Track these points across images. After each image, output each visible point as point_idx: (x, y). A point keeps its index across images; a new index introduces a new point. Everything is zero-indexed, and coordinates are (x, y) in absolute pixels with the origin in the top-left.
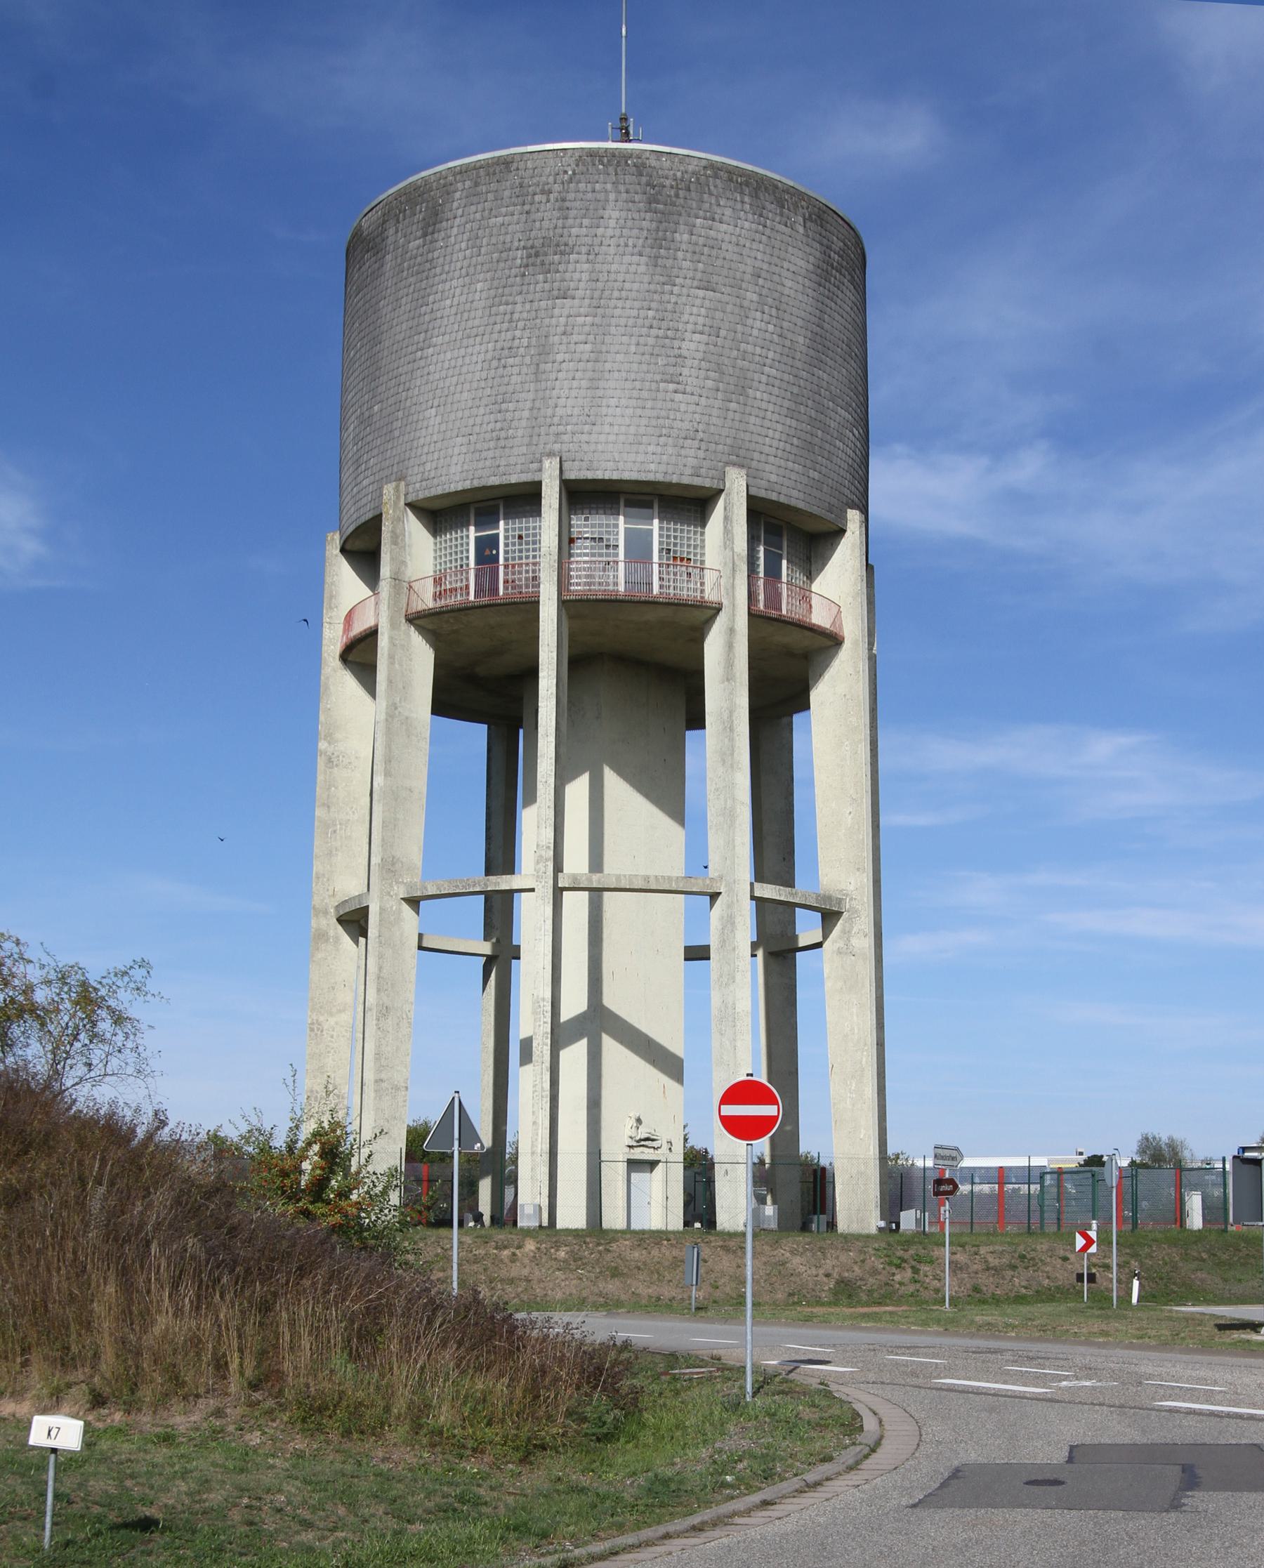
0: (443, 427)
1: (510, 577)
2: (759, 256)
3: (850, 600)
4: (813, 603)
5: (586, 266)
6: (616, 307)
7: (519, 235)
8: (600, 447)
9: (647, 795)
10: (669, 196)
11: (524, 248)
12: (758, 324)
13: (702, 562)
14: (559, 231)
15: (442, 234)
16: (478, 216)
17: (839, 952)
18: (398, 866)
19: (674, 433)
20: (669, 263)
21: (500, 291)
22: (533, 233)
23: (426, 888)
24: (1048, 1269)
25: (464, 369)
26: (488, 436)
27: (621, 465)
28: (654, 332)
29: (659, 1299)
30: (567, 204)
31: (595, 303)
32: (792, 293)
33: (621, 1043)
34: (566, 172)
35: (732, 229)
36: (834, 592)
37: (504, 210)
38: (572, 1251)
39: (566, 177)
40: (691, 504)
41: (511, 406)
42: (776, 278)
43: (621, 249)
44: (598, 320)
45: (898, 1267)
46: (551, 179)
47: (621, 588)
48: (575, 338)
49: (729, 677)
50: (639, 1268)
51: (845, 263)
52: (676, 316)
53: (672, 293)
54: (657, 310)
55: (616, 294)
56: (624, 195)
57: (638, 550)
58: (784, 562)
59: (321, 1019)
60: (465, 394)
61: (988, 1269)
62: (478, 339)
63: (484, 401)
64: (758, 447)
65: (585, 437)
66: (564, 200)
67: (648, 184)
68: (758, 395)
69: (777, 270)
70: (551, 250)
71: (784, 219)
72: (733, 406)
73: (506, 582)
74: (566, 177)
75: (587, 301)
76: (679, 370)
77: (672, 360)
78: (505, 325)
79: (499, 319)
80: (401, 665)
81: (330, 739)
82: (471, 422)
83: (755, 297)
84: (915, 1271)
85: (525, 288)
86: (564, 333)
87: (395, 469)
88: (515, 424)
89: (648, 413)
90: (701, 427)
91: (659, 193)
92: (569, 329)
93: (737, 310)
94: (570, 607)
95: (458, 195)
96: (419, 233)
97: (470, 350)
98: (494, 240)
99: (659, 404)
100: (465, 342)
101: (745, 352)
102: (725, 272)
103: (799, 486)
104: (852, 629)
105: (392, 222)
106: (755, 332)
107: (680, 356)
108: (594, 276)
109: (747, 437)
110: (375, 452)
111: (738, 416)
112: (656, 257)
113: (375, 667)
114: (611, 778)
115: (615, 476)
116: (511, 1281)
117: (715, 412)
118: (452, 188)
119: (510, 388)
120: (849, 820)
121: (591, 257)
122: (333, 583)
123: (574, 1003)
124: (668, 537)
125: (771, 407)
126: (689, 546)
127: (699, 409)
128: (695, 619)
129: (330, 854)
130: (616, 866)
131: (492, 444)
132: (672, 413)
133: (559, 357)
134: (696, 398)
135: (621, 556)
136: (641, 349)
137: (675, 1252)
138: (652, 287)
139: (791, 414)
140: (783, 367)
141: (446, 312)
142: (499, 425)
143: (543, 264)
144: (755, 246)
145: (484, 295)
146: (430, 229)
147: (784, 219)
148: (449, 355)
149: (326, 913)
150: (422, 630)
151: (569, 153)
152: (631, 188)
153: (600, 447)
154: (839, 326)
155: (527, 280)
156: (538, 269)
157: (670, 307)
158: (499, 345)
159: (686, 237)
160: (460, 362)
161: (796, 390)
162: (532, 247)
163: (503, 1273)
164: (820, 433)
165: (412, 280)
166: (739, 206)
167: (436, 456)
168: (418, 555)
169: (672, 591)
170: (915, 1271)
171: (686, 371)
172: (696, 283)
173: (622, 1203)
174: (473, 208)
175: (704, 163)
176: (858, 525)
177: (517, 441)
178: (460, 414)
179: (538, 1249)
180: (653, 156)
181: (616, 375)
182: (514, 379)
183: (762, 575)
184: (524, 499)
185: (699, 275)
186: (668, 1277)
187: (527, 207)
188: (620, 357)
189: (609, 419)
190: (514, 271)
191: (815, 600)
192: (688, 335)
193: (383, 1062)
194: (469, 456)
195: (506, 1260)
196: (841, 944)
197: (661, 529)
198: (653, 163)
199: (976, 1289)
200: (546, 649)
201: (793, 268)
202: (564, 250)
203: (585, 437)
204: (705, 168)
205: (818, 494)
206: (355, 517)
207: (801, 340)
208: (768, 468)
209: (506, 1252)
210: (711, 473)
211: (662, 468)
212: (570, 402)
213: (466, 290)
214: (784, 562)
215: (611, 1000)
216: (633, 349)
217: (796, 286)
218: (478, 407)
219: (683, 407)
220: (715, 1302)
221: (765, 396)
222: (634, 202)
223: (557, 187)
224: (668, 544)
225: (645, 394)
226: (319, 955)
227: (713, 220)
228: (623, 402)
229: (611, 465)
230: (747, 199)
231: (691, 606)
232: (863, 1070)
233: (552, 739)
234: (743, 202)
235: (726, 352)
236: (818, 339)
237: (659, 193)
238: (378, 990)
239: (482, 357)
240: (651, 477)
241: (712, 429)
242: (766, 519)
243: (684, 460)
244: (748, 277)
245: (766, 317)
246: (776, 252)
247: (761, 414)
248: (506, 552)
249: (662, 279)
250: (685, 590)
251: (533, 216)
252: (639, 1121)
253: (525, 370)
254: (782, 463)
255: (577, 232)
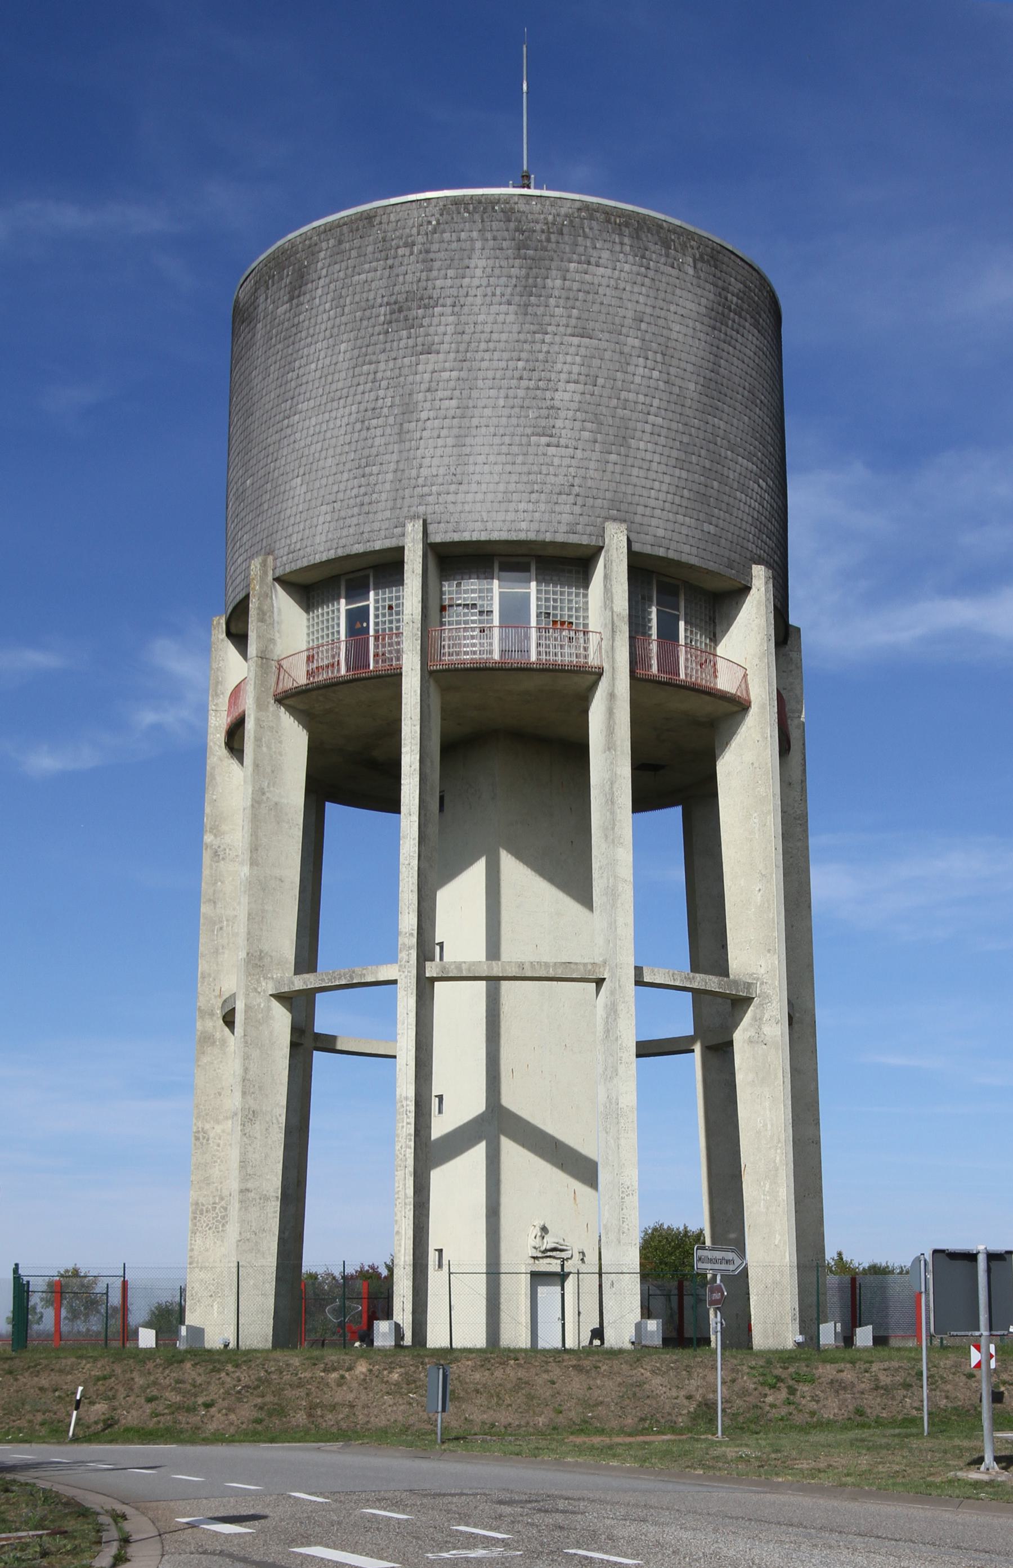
0: (309, 496)
1: (380, 650)
2: (642, 299)
3: (756, 661)
4: (719, 666)
5: (451, 319)
6: (483, 360)
7: (382, 291)
8: (467, 508)
9: (551, 880)
10: (541, 241)
11: (388, 304)
12: (640, 370)
13: (586, 625)
14: (423, 284)
15: (308, 296)
16: (342, 274)
17: (750, 1041)
18: (267, 960)
19: (547, 488)
20: (540, 310)
21: (364, 349)
22: (397, 288)
23: (293, 983)
24: (949, 1387)
25: (328, 435)
26: (352, 502)
27: (489, 525)
28: (524, 383)
29: (493, 1425)
30: (432, 255)
31: (460, 356)
32: (681, 338)
33: (523, 1146)
34: (430, 223)
35: (611, 272)
36: (741, 654)
37: (367, 266)
38: (406, 1373)
39: (430, 228)
40: (568, 564)
41: (375, 469)
42: (661, 322)
43: (488, 299)
44: (463, 374)
45: (773, 1387)
46: (415, 231)
47: (496, 656)
48: (440, 394)
49: (610, 746)
50: (477, 1391)
51: (745, 306)
52: (548, 366)
53: (543, 342)
54: (527, 361)
55: (483, 346)
56: (491, 243)
57: (514, 614)
58: (682, 624)
59: (207, 1126)
60: (329, 460)
61: (877, 1388)
62: (342, 401)
63: (348, 466)
64: (642, 500)
65: (451, 498)
66: (427, 252)
67: (517, 230)
68: (642, 445)
69: (663, 313)
70: (415, 305)
71: (670, 260)
72: (613, 457)
73: (376, 655)
74: (430, 228)
75: (452, 355)
76: (552, 422)
77: (544, 412)
78: (369, 385)
79: (362, 379)
80: (269, 747)
81: (216, 832)
82: (335, 488)
83: (637, 343)
84: (792, 1391)
85: (388, 345)
86: (429, 390)
87: (264, 544)
88: (377, 488)
89: (518, 468)
90: (577, 481)
91: (529, 238)
92: (434, 385)
93: (616, 357)
94: (434, 676)
95: (322, 255)
96: (286, 298)
97: (334, 414)
98: (357, 298)
99: (530, 459)
100: (329, 406)
101: (626, 400)
102: (602, 318)
103: (692, 541)
104: (761, 694)
105: (263, 289)
106: (638, 379)
107: (552, 407)
108: (460, 328)
109: (630, 490)
110: (248, 527)
111: (618, 469)
112: (526, 305)
113: (243, 751)
114: (508, 862)
115: (484, 537)
116: (333, 1408)
117: (592, 465)
118: (317, 248)
119: (374, 451)
120: (758, 898)
121: (456, 309)
122: (218, 669)
123: (461, 1100)
124: (547, 600)
125: (657, 458)
126: (570, 609)
127: (574, 462)
128: (577, 685)
129: (216, 952)
130: (515, 952)
131: (356, 510)
132: (544, 468)
133: (424, 415)
134: (571, 451)
135: (496, 622)
136: (511, 402)
137: (521, 1373)
138: (522, 337)
139: (681, 464)
140: (670, 415)
141: (311, 377)
142: (363, 490)
143: (406, 319)
144: (636, 289)
145: (348, 355)
146: (297, 293)
147: (670, 260)
148: (313, 421)
149: (212, 1014)
150: (292, 710)
151: (433, 202)
152: (499, 234)
153: (467, 508)
154: (738, 371)
155: (390, 337)
156: (401, 324)
157: (541, 356)
158: (362, 407)
159: (558, 283)
160: (324, 427)
161: (686, 439)
162: (395, 303)
163: (327, 1398)
164: (715, 484)
165: (280, 346)
166: (617, 248)
167: (302, 527)
168: (296, 636)
169: (574, 659)
170: (792, 1391)
171: (559, 423)
172: (569, 331)
173: (525, 1318)
174: (337, 267)
175: (577, 205)
176: (763, 580)
177: (381, 506)
178: (324, 481)
179: (370, 1371)
180: (522, 200)
181: (483, 430)
182: (378, 441)
183: (654, 637)
184: (387, 567)
185: (573, 322)
186: (508, 1401)
187: (390, 262)
188: (487, 412)
189: (476, 478)
190: (377, 329)
191: (721, 664)
192: (561, 385)
193: (250, 1170)
194: (333, 525)
195: (333, 1384)
196: (752, 1032)
197: (538, 591)
198: (522, 207)
199: (860, 1412)
200: (409, 722)
201: (681, 311)
202: (428, 302)
203: (451, 498)
204: (579, 209)
205: (715, 549)
206: (234, 597)
207: (692, 386)
208: (654, 522)
209: (334, 1375)
210: (589, 529)
211: (535, 526)
212: (436, 462)
213: (330, 352)
214: (682, 624)
215: (508, 1100)
216: (501, 402)
217: (684, 330)
218: (342, 473)
219: (556, 461)
220: (554, 1429)
221: (650, 446)
222: (501, 249)
223: (420, 239)
224: (547, 607)
225: (515, 449)
226: (205, 1060)
227: (589, 263)
228: (492, 458)
229: (479, 525)
230: (626, 240)
231: (568, 671)
232: (777, 1170)
233: (415, 818)
234: (622, 244)
235: (604, 401)
236: (713, 385)
237: (529, 238)
238: (244, 1093)
239: (345, 420)
240: (522, 536)
241: (590, 483)
242: (646, 573)
243: (559, 517)
244: (628, 322)
245: (649, 363)
246: (662, 295)
247: (646, 465)
248: (376, 624)
249: (532, 328)
250: (566, 656)
251: (395, 271)
252: (544, 1229)
253: (388, 430)
254: (671, 516)
255: (442, 283)
